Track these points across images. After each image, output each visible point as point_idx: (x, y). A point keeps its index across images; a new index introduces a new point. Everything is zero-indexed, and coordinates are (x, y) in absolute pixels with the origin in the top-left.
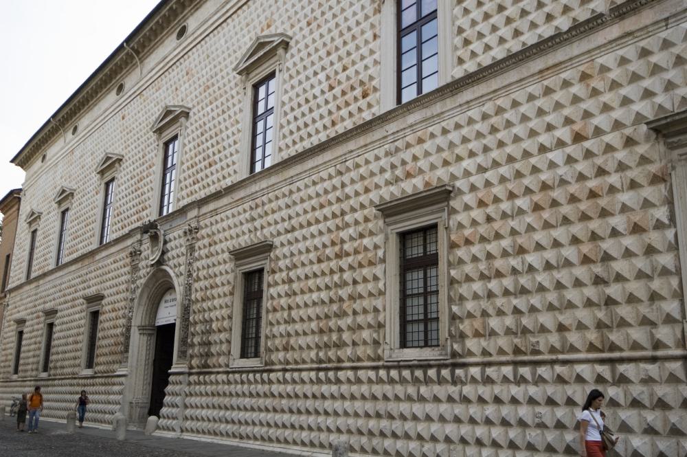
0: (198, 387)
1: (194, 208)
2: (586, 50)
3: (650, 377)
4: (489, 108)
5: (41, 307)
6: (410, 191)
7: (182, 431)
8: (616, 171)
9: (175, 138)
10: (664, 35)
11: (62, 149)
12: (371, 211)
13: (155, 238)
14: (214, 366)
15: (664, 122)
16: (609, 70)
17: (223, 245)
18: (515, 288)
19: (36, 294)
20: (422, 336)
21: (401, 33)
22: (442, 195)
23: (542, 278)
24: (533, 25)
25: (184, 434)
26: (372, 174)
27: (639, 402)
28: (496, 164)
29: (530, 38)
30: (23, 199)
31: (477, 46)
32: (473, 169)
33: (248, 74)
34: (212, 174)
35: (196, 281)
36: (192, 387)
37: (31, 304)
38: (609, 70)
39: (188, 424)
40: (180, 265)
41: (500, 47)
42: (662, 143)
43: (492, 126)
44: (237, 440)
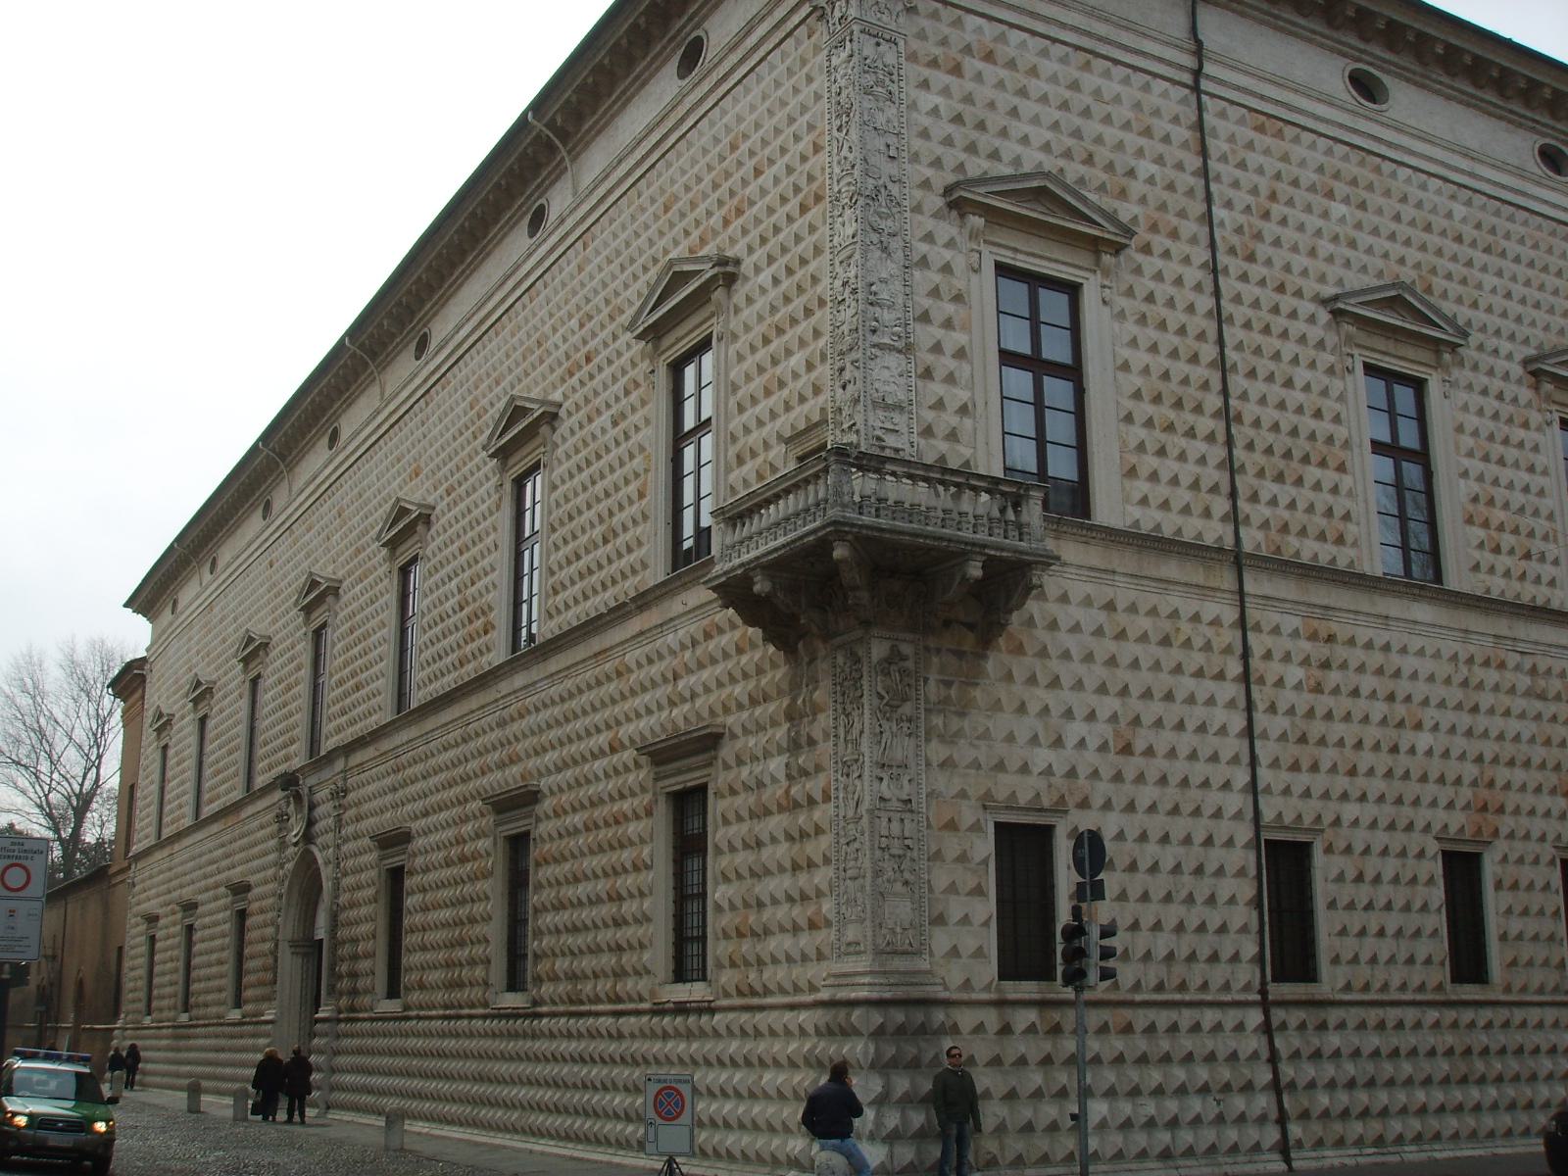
5: (175, 894)
11: (198, 596)
19: (170, 869)
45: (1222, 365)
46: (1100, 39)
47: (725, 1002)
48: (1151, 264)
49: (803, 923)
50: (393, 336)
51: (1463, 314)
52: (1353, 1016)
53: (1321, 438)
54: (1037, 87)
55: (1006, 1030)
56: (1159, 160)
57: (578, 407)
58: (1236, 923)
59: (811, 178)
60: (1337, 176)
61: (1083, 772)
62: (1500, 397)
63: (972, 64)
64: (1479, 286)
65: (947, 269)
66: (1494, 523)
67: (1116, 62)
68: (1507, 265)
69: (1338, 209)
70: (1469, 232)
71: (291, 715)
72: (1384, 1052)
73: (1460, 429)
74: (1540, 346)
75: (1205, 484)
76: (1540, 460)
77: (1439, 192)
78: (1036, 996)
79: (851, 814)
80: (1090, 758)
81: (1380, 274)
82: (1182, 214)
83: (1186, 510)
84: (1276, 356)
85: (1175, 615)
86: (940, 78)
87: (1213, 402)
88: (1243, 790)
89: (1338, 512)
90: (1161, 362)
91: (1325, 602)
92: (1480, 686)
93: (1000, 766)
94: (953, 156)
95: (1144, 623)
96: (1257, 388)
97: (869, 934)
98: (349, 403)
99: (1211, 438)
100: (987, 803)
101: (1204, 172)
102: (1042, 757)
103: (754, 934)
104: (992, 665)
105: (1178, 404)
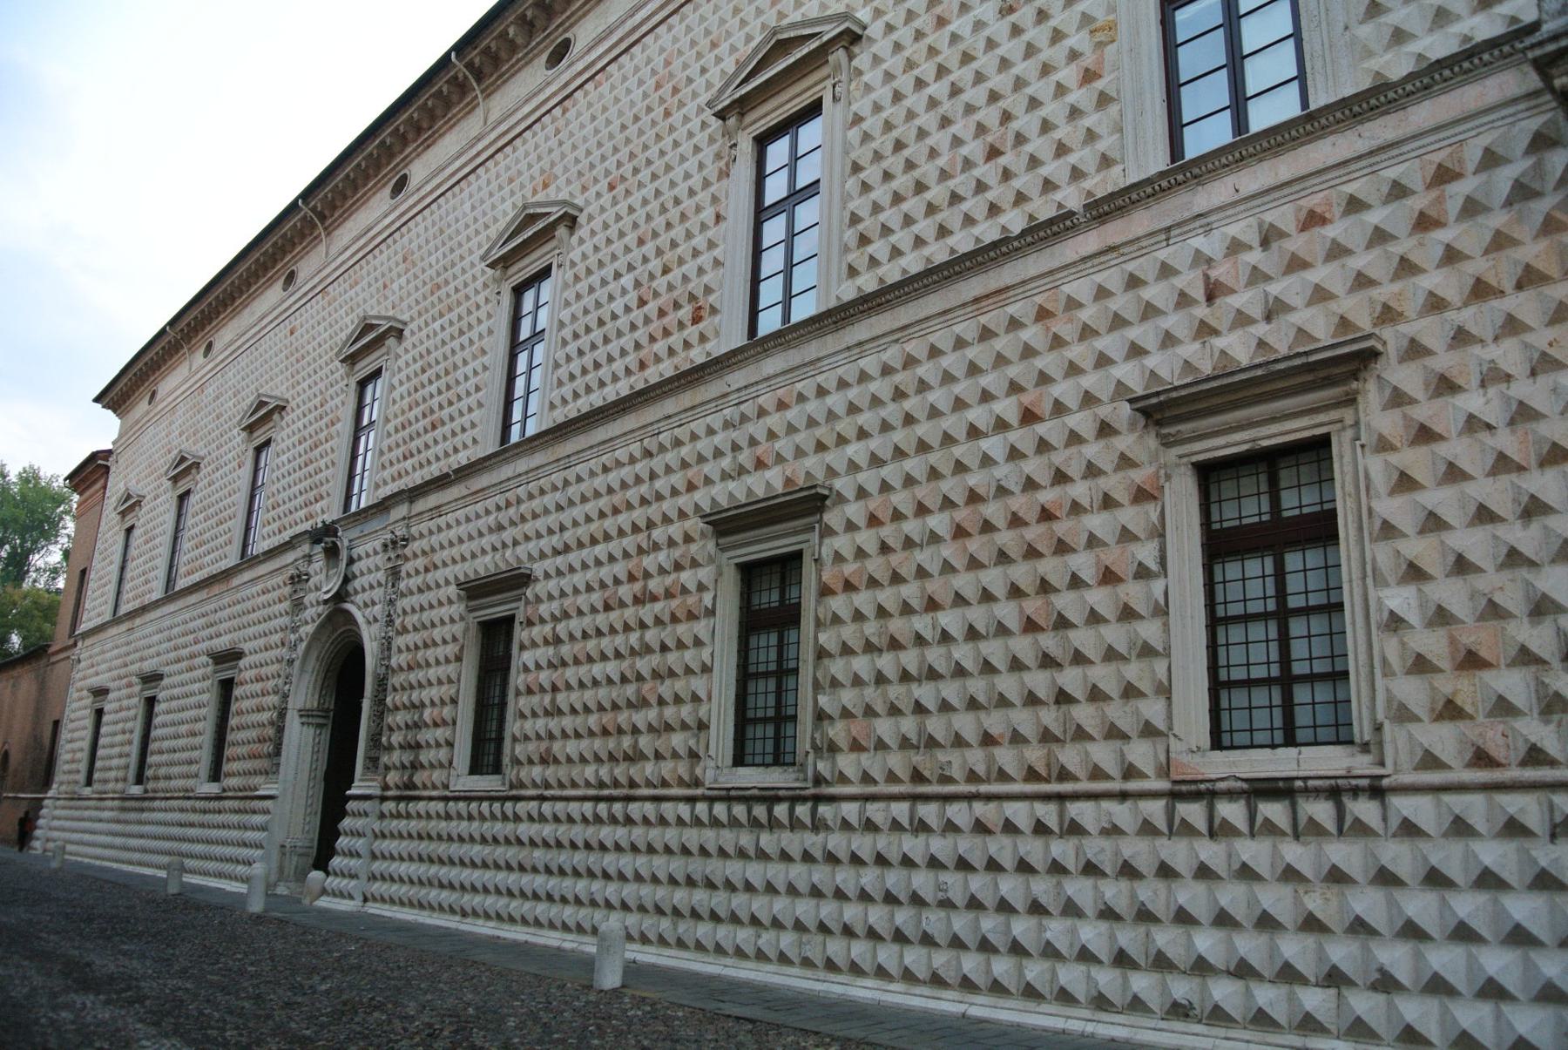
0: (395, 822)
1: (402, 502)
2: (1046, 269)
3: (1115, 826)
4: (892, 355)
5: (135, 668)
6: (760, 492)
7: (366, 900)
8: (1084, 477)
9: (377, 374)
10: (1162, 255)
12: (694, 525)
13: (332, 553)
14: (425, 787)
15: (1154, 401)
16: (1080, 305)
17: (448, 572)
18: (920, 669)
19: (128, 644)
20: (770, 748)
21: (761, 213)
22: (808, 504)
23: (963, 653)
24: (969, 221)
25: (369, 904)
26: (701, 459)
27: (1095, 867)
28: (899, 453)
29: (963, 242)
30: (113, 469)
31: (879, 248)
32: (862, 460)
33: (506, 268)
34: (436, 442)
35: (399, 633)
36: (386, 822)
37: (119, 661)
38: (1080, 305)
39: (377, 887)
40: (374, 603)
41: (916, 254)
42: (1153, 434)
43: (897, 388)
44: (458, 918)
71: (318, 471)
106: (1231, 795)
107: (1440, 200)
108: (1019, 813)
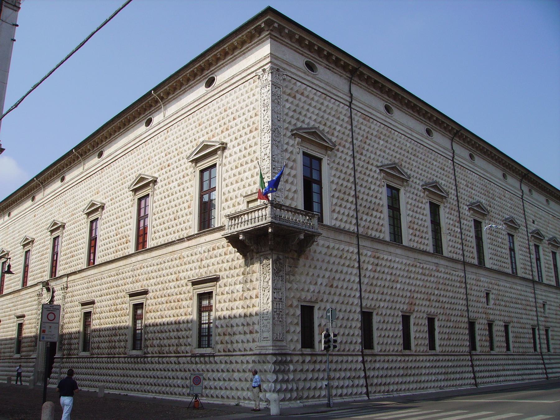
45: (355, 183)
46: (328, 91)
47: (219, 354)
48: (339, 154)
49: (248, 332)
50: (89, 150)
51: (409, 172)
52: (382, 358)
53: (377, 204)
54: (314, 104)
55: (304, 362)
56: (341, 126)
57: (164, 179)
58: (356, 333)
59: (254, 123)
60: (381, 133)
61: (322, 292)
62: (416, 195)
63: (298, 96)
64: (412, 165)
65: (292, 152)
66: (415, 228)
67: (332, 98)
68: (419, 160)
69: (382, 142)
70: (410, 151)
72: (389, 368)
73: (407, 203)
74: (425, 182)
75: (351, 215)
76: (425, 212)
77: (404, 139)
78: (310, 353)
79: (265, 302)
80: (323, 289)
81: (390, 160)
82: (346, 141)
83: (346, 222)
84: (367, 181)
85: (343, 250)
86: (291, 99)
87: (353, 193)
88: (358, 298)
89: (381, 224)
90: (341, 182)
91: (376, 248)
92: (411, 271)
93: (303, 290)
94: (293, 121)
95: (335, 252)
96: (362, 190)
97: (271, 335)
98: (70, 169)
99: (352, 202)
100: (299, 300)
101: (352, 130)
102: (312, 288)
103: (230, 334)
104: (302, 261)
105: (345, 193)
106: (198, 356)
107: (227, 250)
108: (173, 359)
